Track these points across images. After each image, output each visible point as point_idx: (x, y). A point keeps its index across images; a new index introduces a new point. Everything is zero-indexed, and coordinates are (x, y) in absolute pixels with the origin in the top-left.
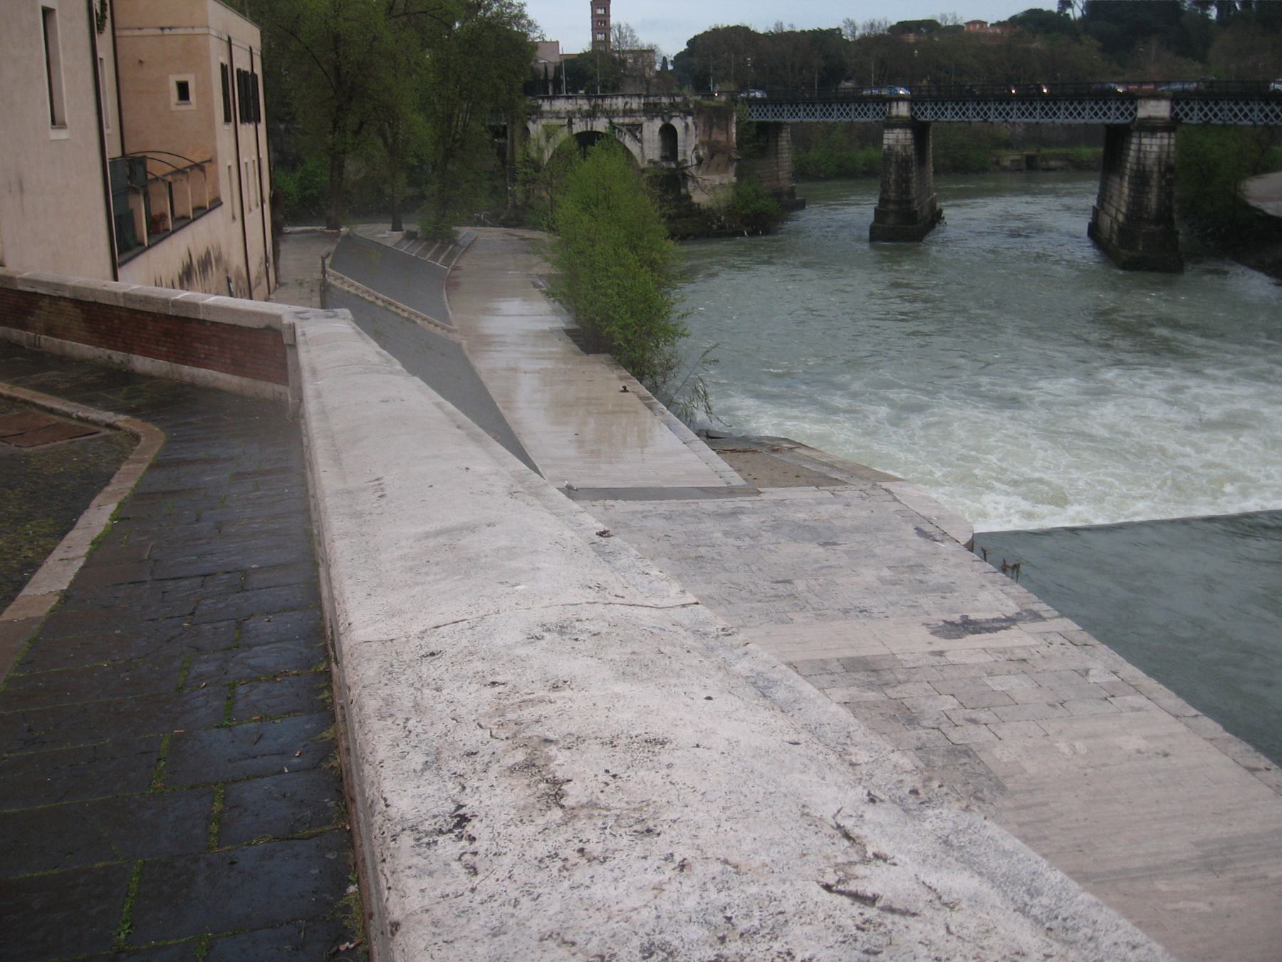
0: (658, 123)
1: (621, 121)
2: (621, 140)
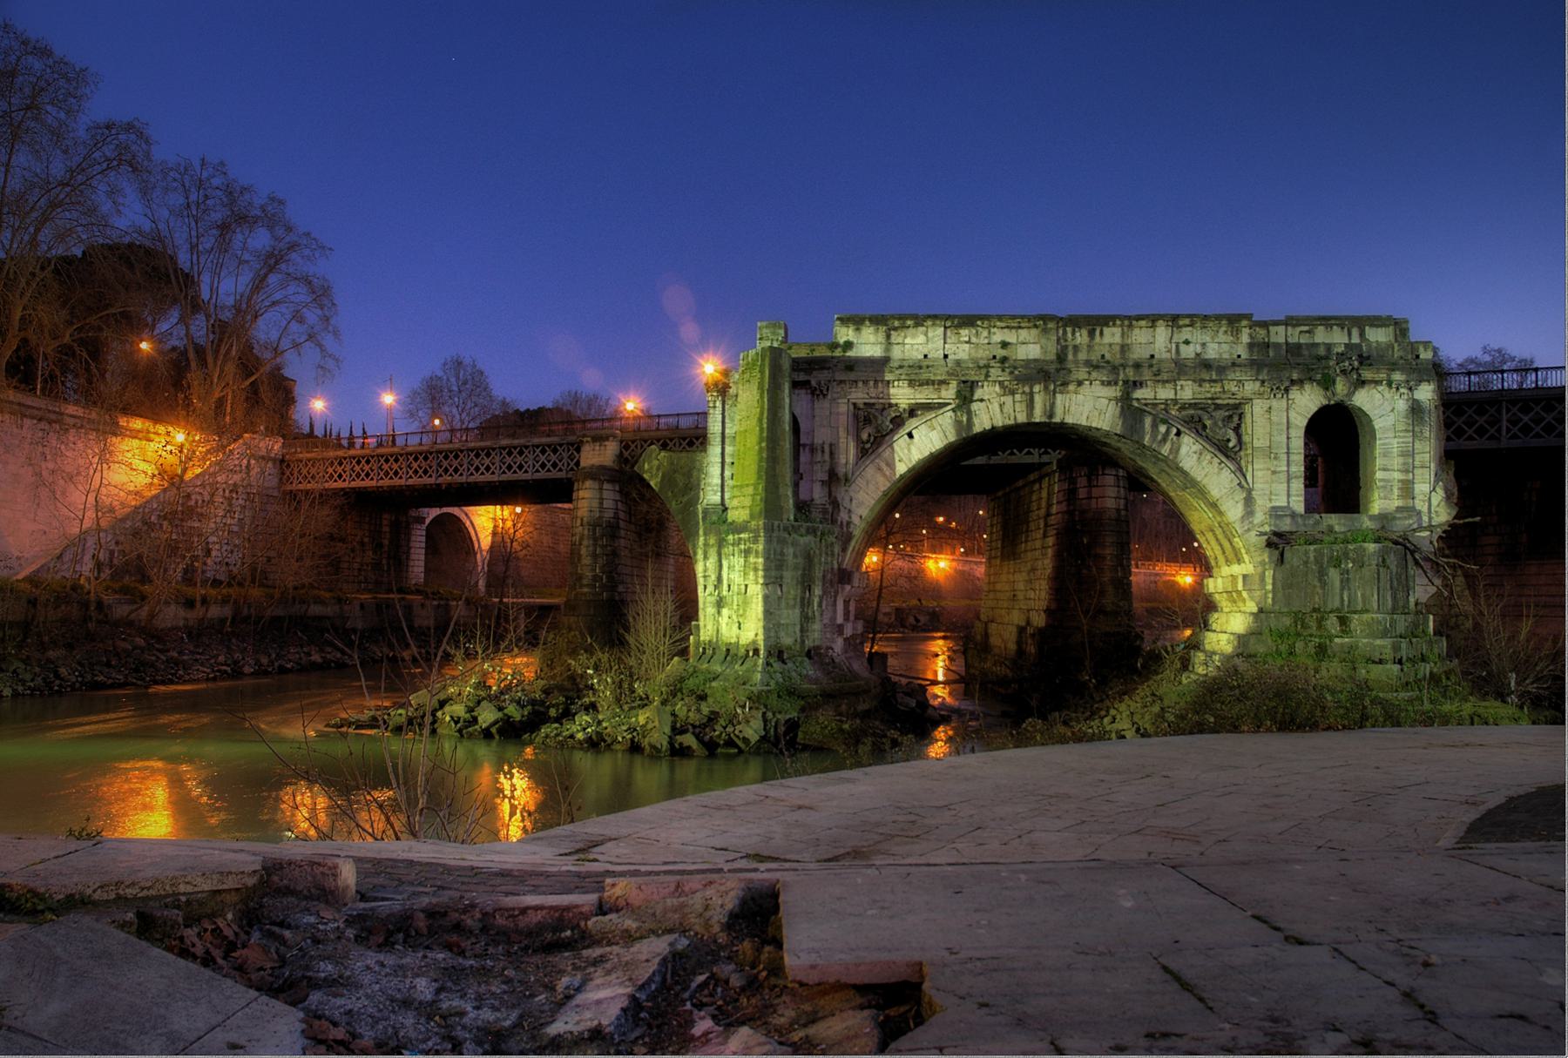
0: (1307, 401)
1: (1165, 393)
2: (1165, 450)
